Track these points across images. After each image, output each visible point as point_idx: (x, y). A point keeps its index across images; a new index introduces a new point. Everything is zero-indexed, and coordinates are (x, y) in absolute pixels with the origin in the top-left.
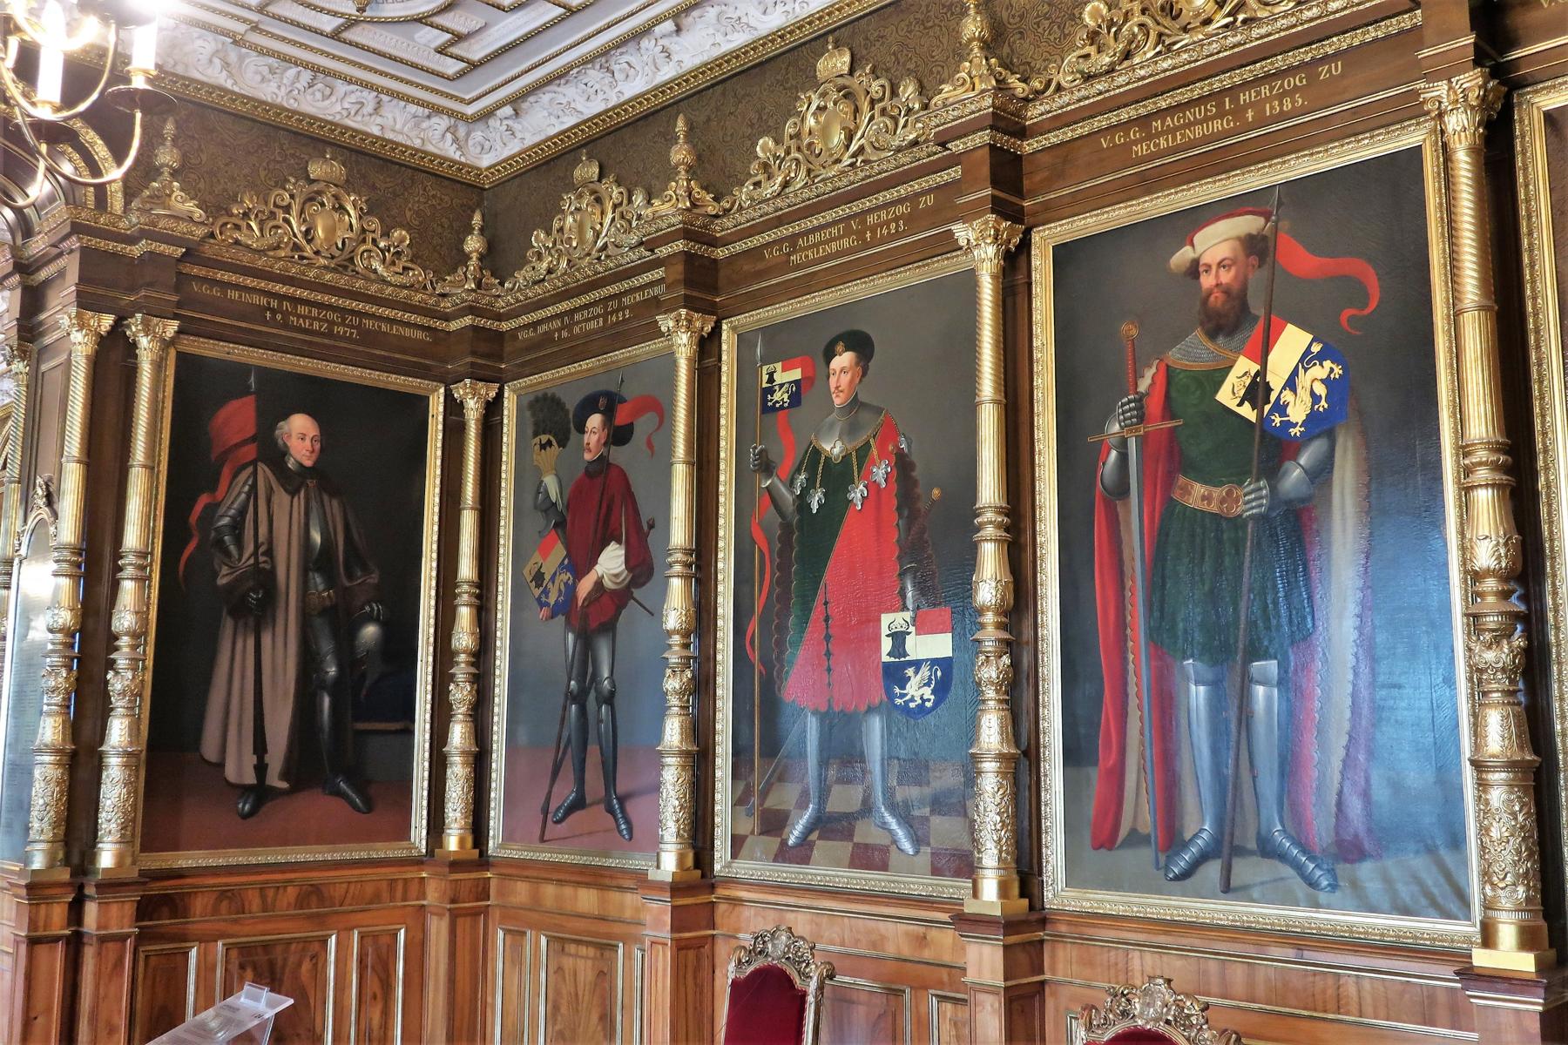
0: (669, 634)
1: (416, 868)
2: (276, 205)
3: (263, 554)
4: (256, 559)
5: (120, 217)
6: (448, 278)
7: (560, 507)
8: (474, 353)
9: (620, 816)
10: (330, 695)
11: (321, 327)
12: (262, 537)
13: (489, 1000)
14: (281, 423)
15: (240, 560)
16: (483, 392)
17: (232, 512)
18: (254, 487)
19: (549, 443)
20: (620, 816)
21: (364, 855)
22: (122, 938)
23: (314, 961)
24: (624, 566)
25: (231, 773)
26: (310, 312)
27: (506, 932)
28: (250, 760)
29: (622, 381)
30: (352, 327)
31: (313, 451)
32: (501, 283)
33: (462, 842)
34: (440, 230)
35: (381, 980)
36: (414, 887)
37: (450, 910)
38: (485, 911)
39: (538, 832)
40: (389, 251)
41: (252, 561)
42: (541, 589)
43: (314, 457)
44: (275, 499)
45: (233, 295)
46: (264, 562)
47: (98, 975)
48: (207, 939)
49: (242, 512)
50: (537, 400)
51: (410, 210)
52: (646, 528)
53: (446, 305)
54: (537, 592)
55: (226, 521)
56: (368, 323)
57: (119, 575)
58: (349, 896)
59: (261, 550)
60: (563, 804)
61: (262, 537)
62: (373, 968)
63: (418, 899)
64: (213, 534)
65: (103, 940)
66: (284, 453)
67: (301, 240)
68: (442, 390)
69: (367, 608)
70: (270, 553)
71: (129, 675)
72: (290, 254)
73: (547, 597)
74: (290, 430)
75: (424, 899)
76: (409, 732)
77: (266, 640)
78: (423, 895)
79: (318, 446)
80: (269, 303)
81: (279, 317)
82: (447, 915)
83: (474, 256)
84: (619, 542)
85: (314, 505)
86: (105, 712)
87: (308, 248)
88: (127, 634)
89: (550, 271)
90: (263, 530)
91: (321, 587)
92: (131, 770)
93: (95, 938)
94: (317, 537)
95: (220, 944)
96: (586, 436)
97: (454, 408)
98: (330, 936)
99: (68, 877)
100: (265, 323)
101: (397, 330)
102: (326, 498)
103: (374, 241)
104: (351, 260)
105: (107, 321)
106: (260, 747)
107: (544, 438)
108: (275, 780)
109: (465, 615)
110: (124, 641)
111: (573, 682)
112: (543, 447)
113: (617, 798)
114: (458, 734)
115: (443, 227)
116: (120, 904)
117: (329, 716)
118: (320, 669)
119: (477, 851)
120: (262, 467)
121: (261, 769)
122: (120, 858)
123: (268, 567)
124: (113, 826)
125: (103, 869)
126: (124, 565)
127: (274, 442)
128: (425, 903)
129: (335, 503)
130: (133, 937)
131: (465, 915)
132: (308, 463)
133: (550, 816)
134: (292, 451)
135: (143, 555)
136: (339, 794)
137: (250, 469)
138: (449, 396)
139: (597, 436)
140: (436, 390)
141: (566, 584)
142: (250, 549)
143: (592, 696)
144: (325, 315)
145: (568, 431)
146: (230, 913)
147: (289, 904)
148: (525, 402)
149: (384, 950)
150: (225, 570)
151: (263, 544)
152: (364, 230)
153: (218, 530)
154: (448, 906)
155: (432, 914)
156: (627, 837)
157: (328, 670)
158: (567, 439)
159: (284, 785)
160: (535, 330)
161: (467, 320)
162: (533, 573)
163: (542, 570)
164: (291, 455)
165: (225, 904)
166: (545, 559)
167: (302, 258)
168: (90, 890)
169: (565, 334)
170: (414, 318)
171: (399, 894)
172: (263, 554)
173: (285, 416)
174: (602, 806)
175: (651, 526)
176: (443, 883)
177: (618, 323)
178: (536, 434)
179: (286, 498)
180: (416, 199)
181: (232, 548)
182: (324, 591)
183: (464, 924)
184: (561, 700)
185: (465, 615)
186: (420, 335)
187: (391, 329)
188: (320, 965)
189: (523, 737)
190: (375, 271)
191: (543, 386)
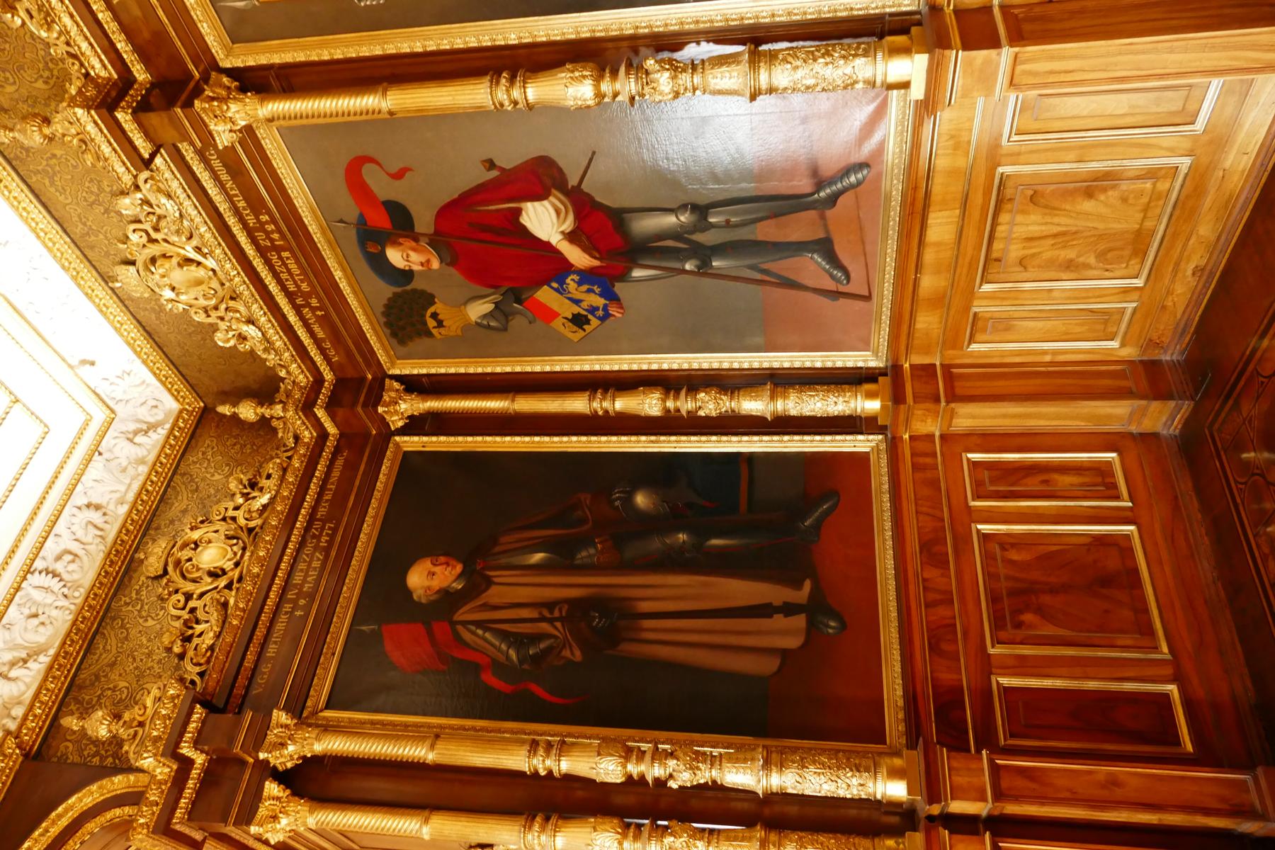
0: (600, 95)
1: (900, 445)
2: (183, 609)
3: (552, 613)
4: (556, 619)
5: (154, 777)
6: (280, 435)
7: (497, 297)
8: (354, 404)
9: (839, 185)
10: (708, 539)
11: (319, 559)
12: (534, 614)
13: (1048, 358)
14: (415, 598)
15: (556, 637)
16: (393, 394)
17: (504, 647)
18: (479, 624)
19: (434, 316)
20: (839, 185)
21: (886, 497)
22: (995, 770)
23: (1006, 546)
24: (545, 203)
25: (793, 642)
26: (302, 570)
27: (971, 340)
28: (779, 621)
29: (341, 221)
30: (323, 529)
31: (448, 564)
32: (283, 380)
33: (870, 395)
34: (238, 447)
35: (1024, 477)
36: (921, 446)
37: (948, 402)
38: (947, 368)
39: (859, 305)
40: (248, 494)
41: (558, 624)
42: (590, 317)
43: (452, 562)
44: (496, 601)
45: (271, 650)
46: (561, 612)
47: (1042, 799)
48: (987, 666)
49: (504, 635)
50: (394, 334)
51: (213, 475)
53: (307, 435)
54: (594, 322)
55: (512, 654)
56: (322, 512)
57: (556, 774)
58: (930, 511)
59: (548, 615)
60: (827, 271)
61: (534, 614)
62: (1011, 485)
63: (934, 442)
64: (525, 667)
65: (999, 795)
66: (445, 593)
67: (222, 582)
68: (397, 438)
69: (617, 503)
70: (550, 605)
71: (672, 763)
72: (233, 593)
73: (597, 309)
74: (422, 587)
75: (933, 436)
76: (750, 458)
77: (646, 606)
78: (930, 437)
79: (442, 559)
80: (286, 613)
81: (302, 602)
82: (953, 405)
83: (260, 410)
84: (518, 212)
85: (504, 560)
86: (716, 787)
87: (230, 574)
88: (624, 767)
89: (250, 321)
90: (525, 613)
91: (592, 551)
92: (786, 759)
93: (996, 804)
94: (538, 557)
95: (991, 651)
96: (416, 268)
97: (415, 425)
98: (978, 531)
99: (917, 833)
100: (307, 616)
101: (332, 484)
102: (497, 549)
103: (236, 508)
104: (250, 530)
105: (272, 788)
106: (764, 610)
107: (431, 323)
108: (802, 594)
109: (622, 404)
110: (634, 769)
111: (688, 267)
112: (440, 324)
113: (818, 191)
114: (752, 405)
115: (235, 445)
116: (953, 773)
117: (732, 539)
118: (683, 547)
119: (880, 379)
120: (459, 616)
121: (789, 609)
122: (895, 774)
123: (566, 607)
124: (855, 781)
125: (909, 793)
126: (545, 769)
127: (432, 604)
128: (937, 434)
129: (503, 540)
130: (994, 756)
131: (953, 388)
132: (459, 568)
133: (841, 289)
134: (445, 584)
135: (534, 746)
136: (817, 526)
137: (459, 627)
138: (404, 431)
140: (397, 445)
141: (580, 283)
142: (545, 627)
143: (699, 237)
144: (307, 555)
145: (414, 291)
146: (956, 641)
147: (942, 575)
148: (402, 350)
149: (996, 473)
150: (566, 653)
151: (540, 613)
152: (224, 519)
153: (521, 662)
154: (943, 404)
155: (950, 425)
156: (865, 172)
157: (681, 541)
159: (807, 585)
160: (323, 340)
161: (320, 413)
162: (575, 328)
163: (570, 317)
164: (449, 586)
165: (945, 646)
166: (556, 315)
167: (240, 580)
168: (935, 810)
169: (314, 302)
170: (321, 468)
171: (928, 460)
172: (552, 613)
173: (408, 593)
174: (829, 213)
175: (490, 164)
176: (916, 412)
177: (279, 231)
178: (429, 334)
179: (494, 590)
180: (203, 470)
181: (542, 646)
182: (596, 548)
183: (960, 388)
184: (707, 281)
185: (622, 404)
186: (340, 462)
187: (330, 490)
188: (1012, 541)
189: (759, 340)
190: (265, 507)
191: (377, 327)
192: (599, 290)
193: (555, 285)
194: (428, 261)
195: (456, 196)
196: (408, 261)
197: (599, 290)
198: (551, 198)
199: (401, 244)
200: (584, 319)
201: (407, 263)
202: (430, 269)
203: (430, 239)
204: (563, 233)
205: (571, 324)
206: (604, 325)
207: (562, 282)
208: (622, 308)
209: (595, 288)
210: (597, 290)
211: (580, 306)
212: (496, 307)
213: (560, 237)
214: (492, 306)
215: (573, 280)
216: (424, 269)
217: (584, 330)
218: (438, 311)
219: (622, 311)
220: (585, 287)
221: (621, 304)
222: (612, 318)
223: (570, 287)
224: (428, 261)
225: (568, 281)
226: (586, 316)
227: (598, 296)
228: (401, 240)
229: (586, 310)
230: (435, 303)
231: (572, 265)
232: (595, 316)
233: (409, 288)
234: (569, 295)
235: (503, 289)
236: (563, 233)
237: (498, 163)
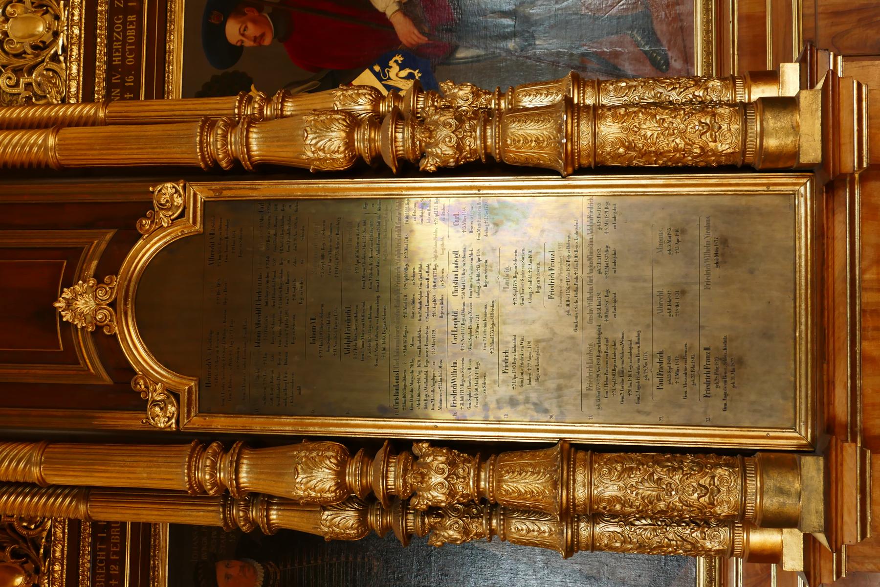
96: (248, 43)
126: (226, 154)
139: (250, 26)
141: (402, 67)
192: (420, 75)
193: (377, 68)
194: (263, 36)
196: (243, 35)
199: (245, 14)
201: (241, 38)
207: (385, 66)
209: (416, 73)
215: (396, 61)
216: (255, 45)
220: (404, 73)
224: (263, 36)
225: (391, 63)
233: (230, 70)
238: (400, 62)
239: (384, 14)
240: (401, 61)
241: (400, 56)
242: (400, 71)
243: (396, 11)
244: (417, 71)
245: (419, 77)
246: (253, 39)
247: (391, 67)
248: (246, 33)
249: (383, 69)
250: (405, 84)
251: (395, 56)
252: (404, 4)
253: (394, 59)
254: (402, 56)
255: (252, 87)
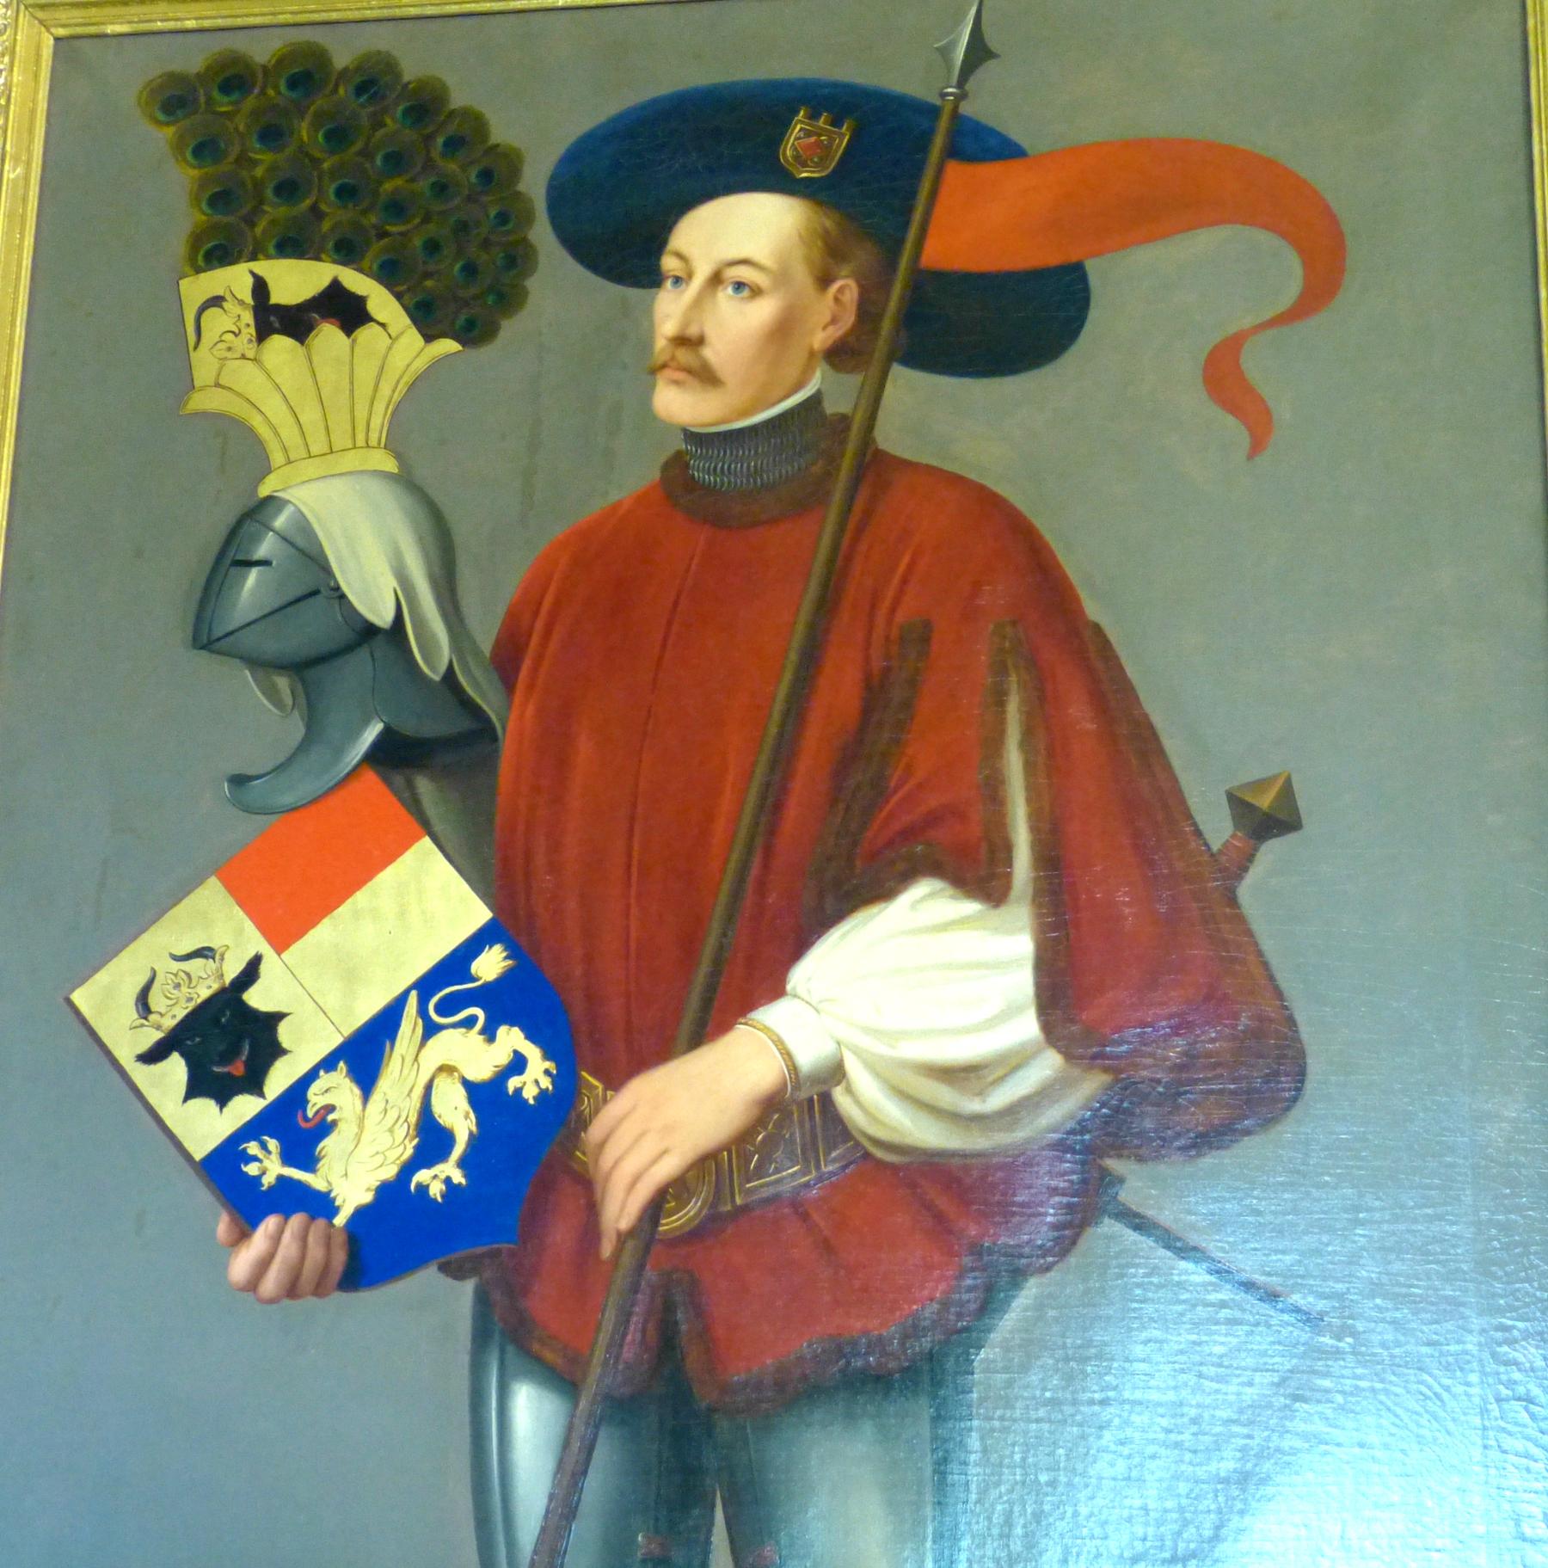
24: (1028, 1027)
29: (979, 52)
42: (246, 1107)
52: (1217, 827)
139: (763, 311)
141: (484, 1096)
145: (519, 259)
158: (508, 299)
162: (171, 1011)
192: (436, 1190)
193: (490, 965)
194: (706, 377)
195: (1092, 609)
196: (716, 279)
197: (436, 1190)
198: (1049, 1064)
200: (238, 1069)
201: (702, 273)
202: (654, 371)
203: (844, 421)
204: (836, 1072)
205: (204, 993)
206: (189, 1171)
208: (292, 1290)
210: (435, 1179)
211: (328, 1063)
212: (369, 631)
213: (809, 1057)
214: (382, 616)
215: (518, 1064)
216: (660, 343)
217: (153, 1056)
218: (365, 333)
219: (271, 1283)
221: (319, 1290)
222: (223, 1225)
223: (474, 1037)
224: (706, 377)
225: (511, 1039)
226: (254, 1084)
227: (390, 1172)
228: (847, 288)
229: (297, 1093)
230: (429, 338)
231: (615, 1081)
232: (253, 1129)
233: (542, 234)
234: (410, 1024)
235: (482, 690)
236: (836, 1072)
237: (1272, 851)
238: (513, 1083)
239: (777, 990)
240: (518, 1091)
241: (546, 1083)
242: (467, 1084)
243: (787, 1056)
244: (458, 1178)
245: (423, 1189)
246: (693, 331)
247: (489, 1034)
248: (725, 294)
249: (487, 996)
250: (392, 1115)
251: (547, 1056)
252: (826, 1100)
253: (532, 1052)
254: (542, 1095)
255: (448, 346)
